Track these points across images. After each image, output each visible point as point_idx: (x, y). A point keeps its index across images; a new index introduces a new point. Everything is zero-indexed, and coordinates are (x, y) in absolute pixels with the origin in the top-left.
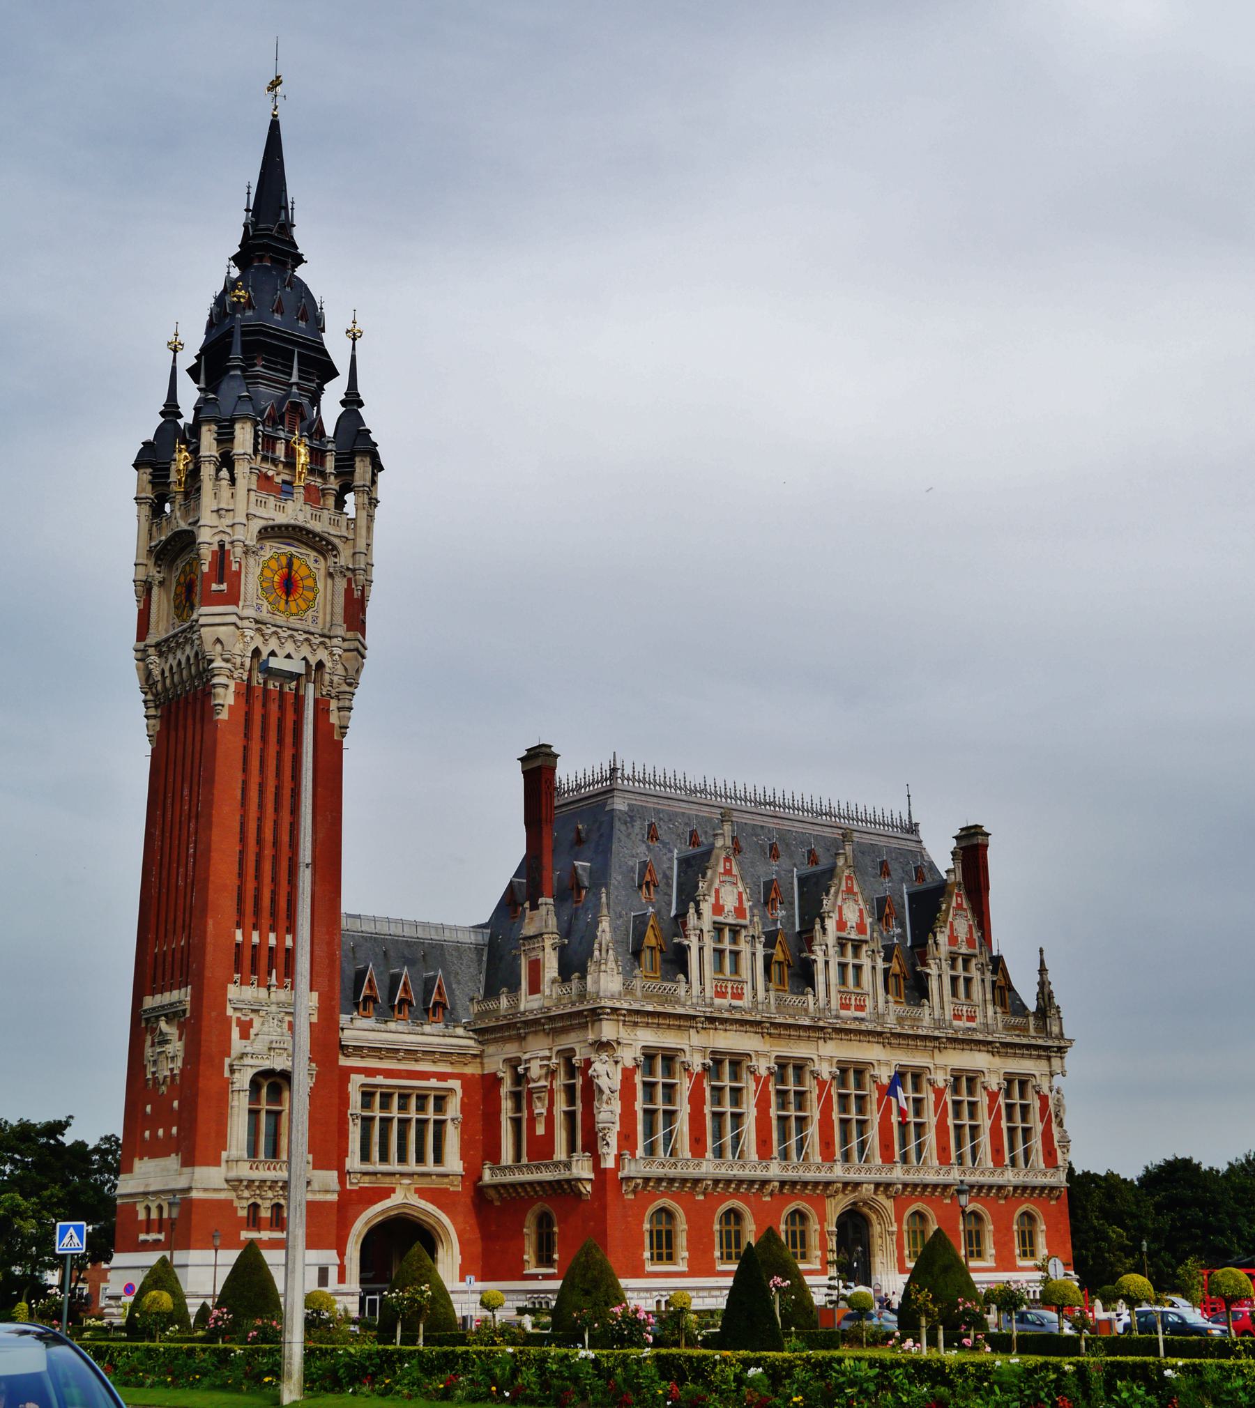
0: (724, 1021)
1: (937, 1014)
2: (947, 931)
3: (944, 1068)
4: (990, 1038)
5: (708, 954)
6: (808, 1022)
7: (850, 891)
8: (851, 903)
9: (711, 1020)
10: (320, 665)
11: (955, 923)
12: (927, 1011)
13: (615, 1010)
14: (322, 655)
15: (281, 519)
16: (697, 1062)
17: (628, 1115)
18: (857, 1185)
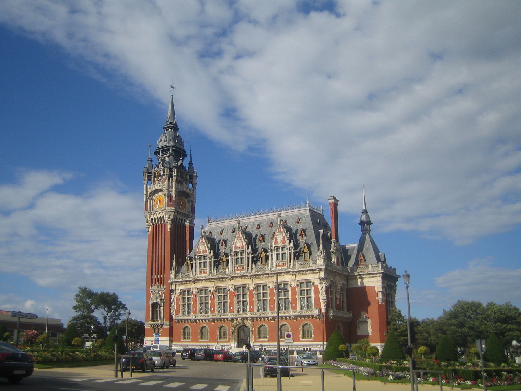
0: (199, 280)
1: (270, 266)
2: (274, 240)
3: (273, 282)
4: (287, 271)
5: (198, 265)
6: (222, 277)
7: (239, 237)
8: (239, 240)
9: (197, 280)
10: (163, 217)
11: (278, 238)
12: (267, 266)
13: (172, 282)
14: (164, 214)
15: (154, 189)
16: (195, 291)
17: (178, 306)
18: (237, 319)
